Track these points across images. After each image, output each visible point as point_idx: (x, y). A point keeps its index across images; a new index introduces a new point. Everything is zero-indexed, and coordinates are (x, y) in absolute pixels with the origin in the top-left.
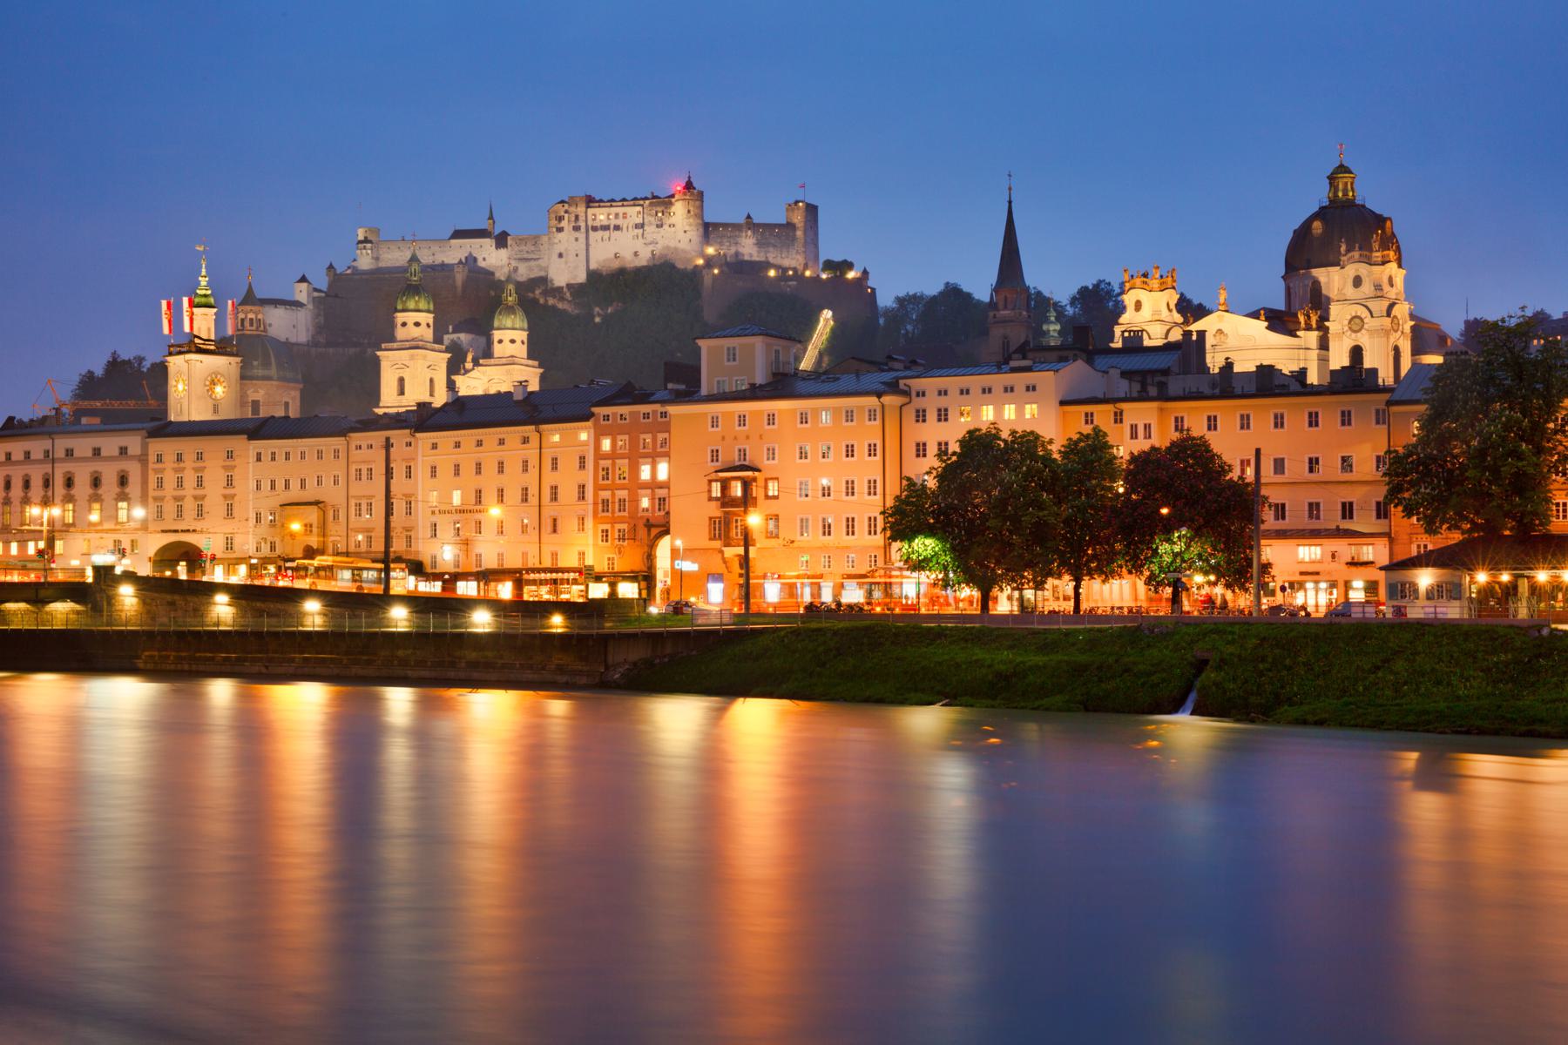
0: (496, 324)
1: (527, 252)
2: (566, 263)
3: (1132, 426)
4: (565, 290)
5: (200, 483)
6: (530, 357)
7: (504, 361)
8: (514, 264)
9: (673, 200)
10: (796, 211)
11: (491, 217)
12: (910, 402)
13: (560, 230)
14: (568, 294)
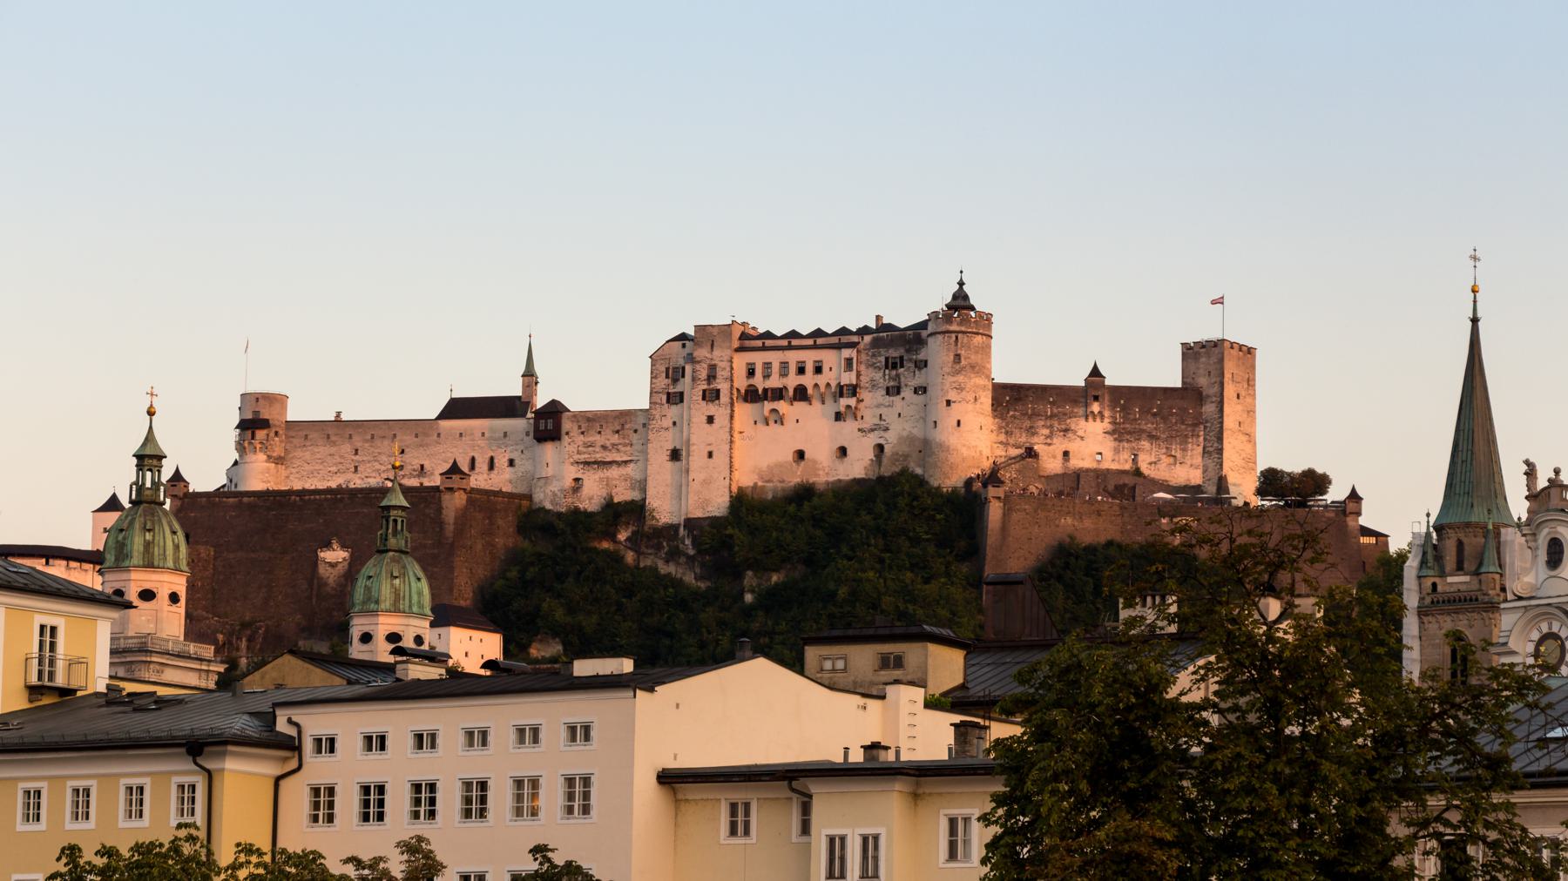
1: (604, 447)
3: (832, 840)
4: (682, 529)
9: (924, 333)
10: (1203, 360)
11: (529, 374)
12: (300, 767)
13: (676, 398)
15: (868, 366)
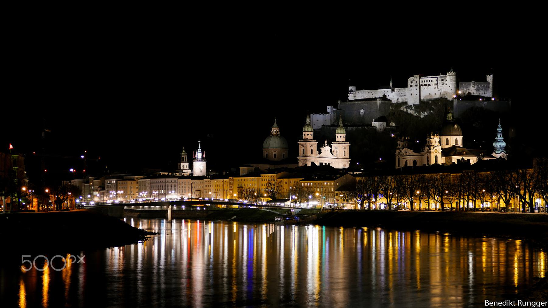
0: (336, 132)
1: (401, 94)
2: (413, 97)
4: (413, 106)
5: (185, 187)
6: (346, 141)
7: (338, 142)
8: (397, 97)
13: (411, 86)
14: (413, 108)
15: (439, 80)
